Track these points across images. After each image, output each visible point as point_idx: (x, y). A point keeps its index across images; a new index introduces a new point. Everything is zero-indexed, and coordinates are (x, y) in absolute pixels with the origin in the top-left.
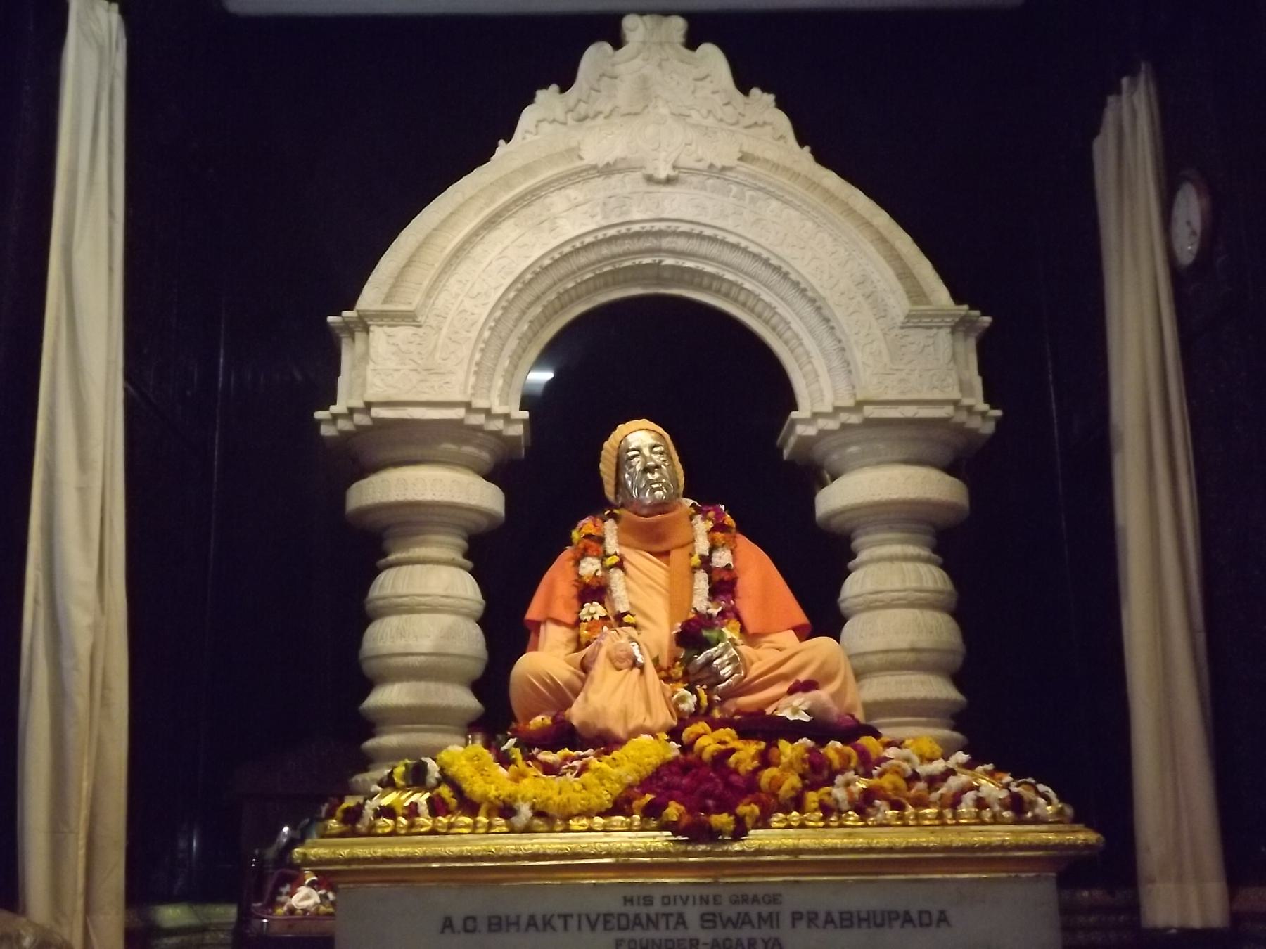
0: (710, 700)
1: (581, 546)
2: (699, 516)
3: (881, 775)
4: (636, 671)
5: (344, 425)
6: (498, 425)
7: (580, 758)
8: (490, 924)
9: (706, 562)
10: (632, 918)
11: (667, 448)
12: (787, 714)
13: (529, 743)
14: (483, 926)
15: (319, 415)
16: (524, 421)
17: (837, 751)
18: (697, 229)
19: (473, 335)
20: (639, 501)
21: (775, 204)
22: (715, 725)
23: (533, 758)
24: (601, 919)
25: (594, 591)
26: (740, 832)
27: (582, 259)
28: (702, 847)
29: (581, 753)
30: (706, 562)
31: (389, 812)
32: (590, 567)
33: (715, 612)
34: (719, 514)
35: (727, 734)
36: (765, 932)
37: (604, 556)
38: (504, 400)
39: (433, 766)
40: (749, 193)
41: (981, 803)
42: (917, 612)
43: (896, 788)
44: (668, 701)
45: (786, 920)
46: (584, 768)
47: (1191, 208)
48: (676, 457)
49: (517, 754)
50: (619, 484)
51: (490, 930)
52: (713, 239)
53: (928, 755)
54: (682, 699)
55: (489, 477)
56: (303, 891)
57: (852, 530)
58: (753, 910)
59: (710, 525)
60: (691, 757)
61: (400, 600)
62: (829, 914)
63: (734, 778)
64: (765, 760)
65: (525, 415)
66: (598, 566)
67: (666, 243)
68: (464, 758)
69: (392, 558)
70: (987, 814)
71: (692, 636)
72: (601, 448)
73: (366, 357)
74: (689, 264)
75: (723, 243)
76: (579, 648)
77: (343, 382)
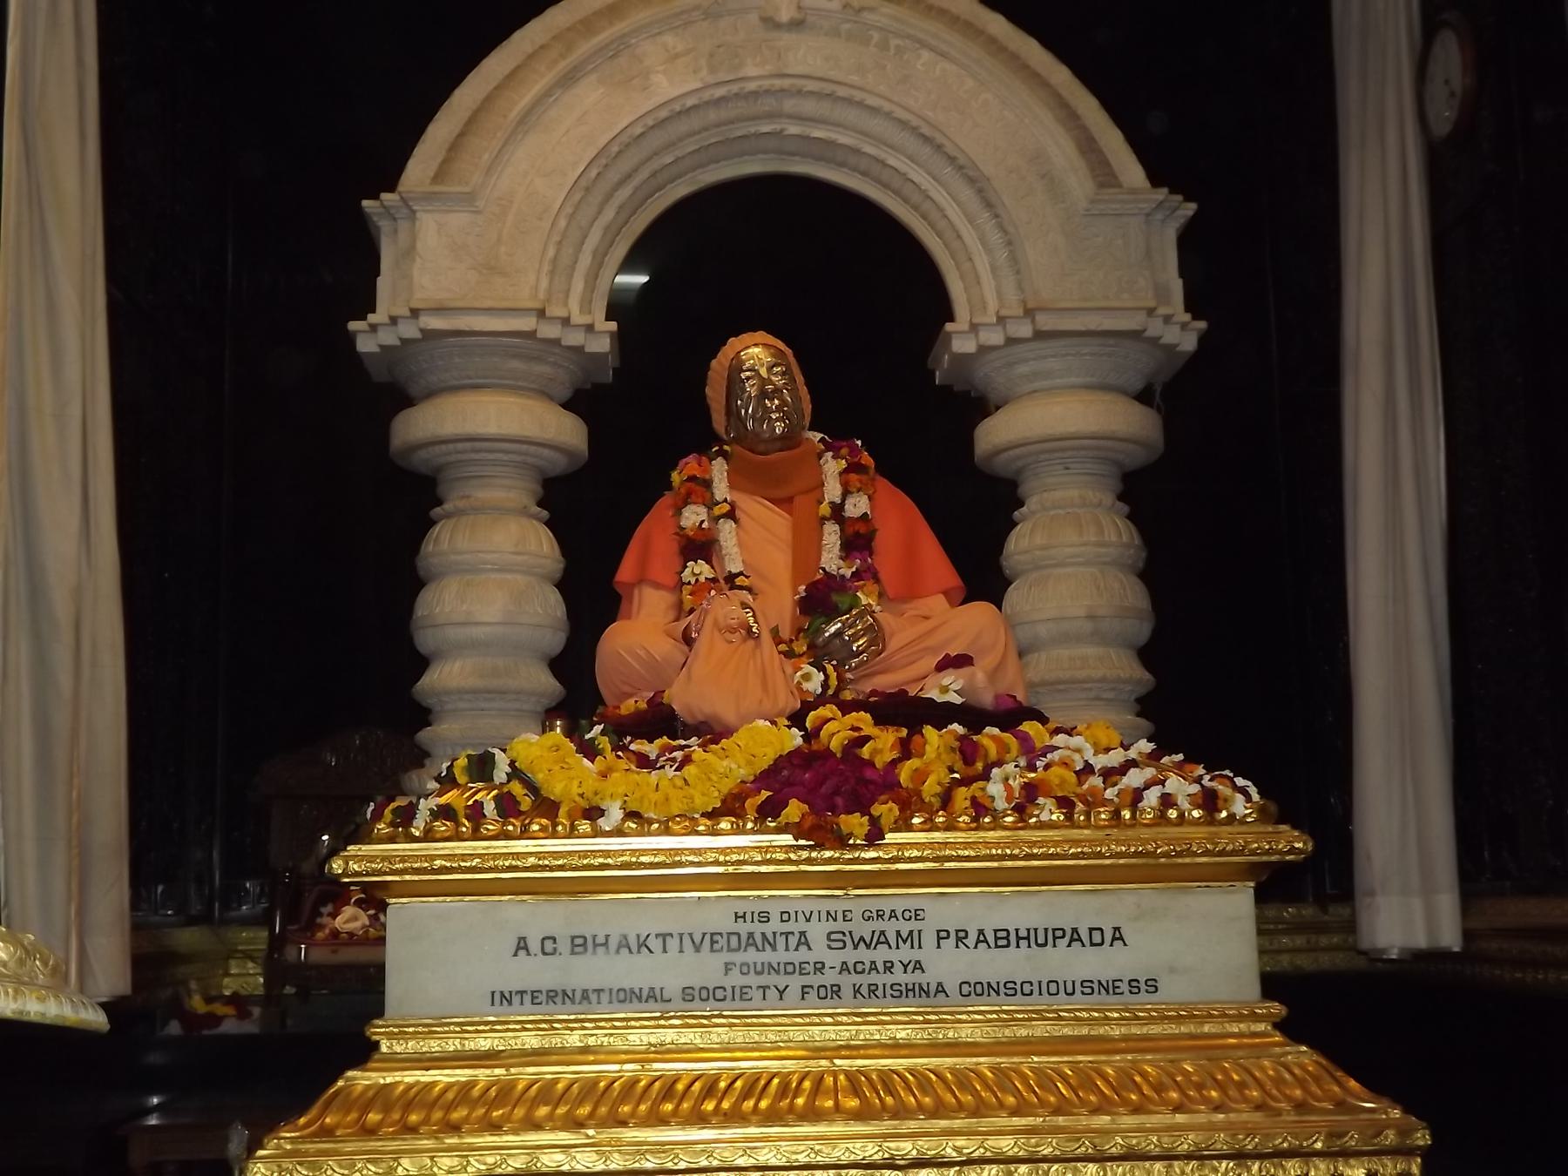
0: (840, 678)
1: (683, 491)
3: (1047, 767)
4: (751, 643)
5: (388, 338)
6: (574, 338)
7: (682, 748)
8: (574, 945)
9: (837, 511)
10: (744, 938)
11: (788, 367)
12: (934, 695)
13: (622, 730)
14: (564, 946)
15: (353, 325)
16: (612, 334)
17: (993, 738)
18: (828, 88)
19: (547, 225)
20: (755, 434)
21: (926, 55)
22: (846, 708)
23: (625, 748)
24: (708, 937)
25: (700, 547)
26: (874, 836)
27: (683, 126)
28: (828, 854)
29: (683, 742)
30: (837, 511)
31: (445, 812)
32: (693, 516)
33: (848, 573)
34: (854, 451)
35: (863, 719)
36: (906, 953)
37: (711, 504)
38: (586, 305)
40: (894, 42)
41: (1167, 801)
43: (1063, 781)
44: (788, 679)
45: (929, 939)
46: (687, 760)
47: (1450, 58)
48: (800, 379)
49: (604, 743)
50: (732, 411)
51: (573, 953)
52: (849, 101)
53: (1104, 743)
54: (807, 677)
55: (567, 406)
56: (349, 911)
57: (1020, 471)
58: (890, 928)
60: (815, 747)
61: (459, 558)
62: (981, 932)
63: (868, 774)
64: (906, 750)
65: (613, 326)
66: (704, 517)
67: (789, 105)
68: (541, 751)
69: (448, 506)
70: (1172, 814)
71: (820, 599)
72: (708, 368)
73: (410, 252)
74: (818, 133)
75: (861, 105)
76: (680, 611)
77: (383, 284)
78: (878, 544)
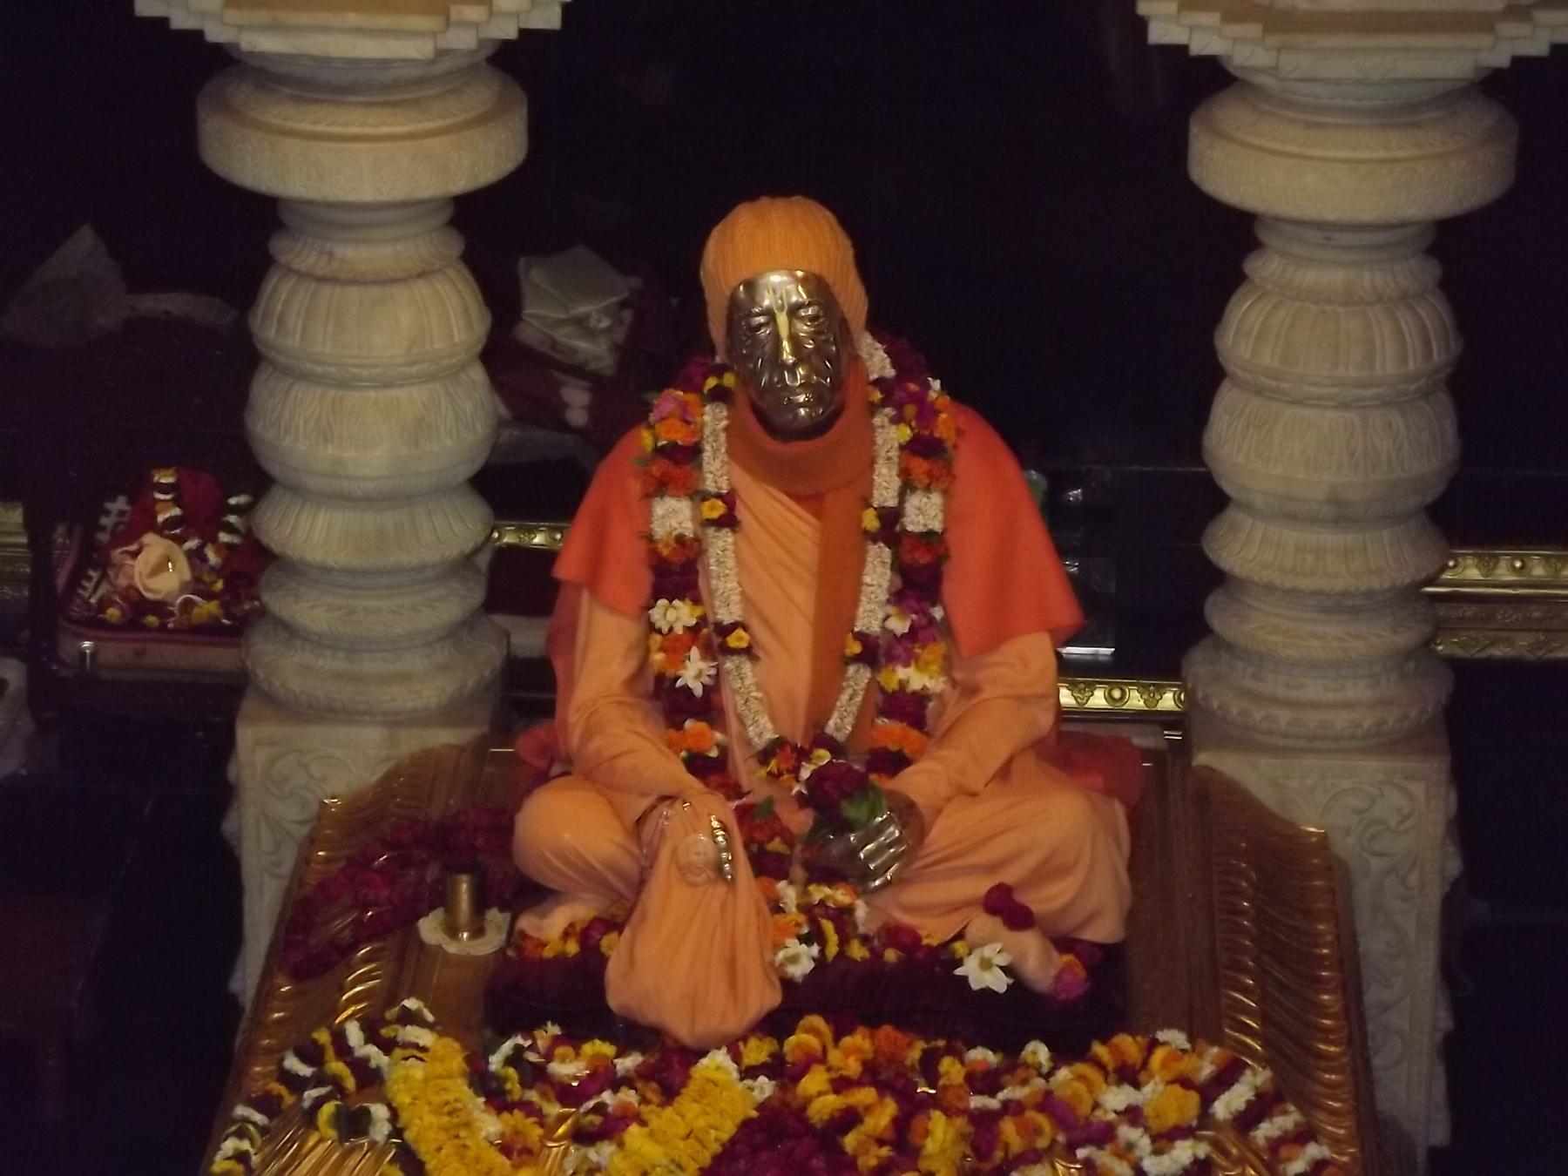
2: (889, 411)
4: (721, 889)
9: (890, 518)
25: (677, 574)
32: (673, 516)
39: (379, 1111)
42: (1353, 416)
56: (154, 546)
59: (904, 433)
78: (949, 588)
